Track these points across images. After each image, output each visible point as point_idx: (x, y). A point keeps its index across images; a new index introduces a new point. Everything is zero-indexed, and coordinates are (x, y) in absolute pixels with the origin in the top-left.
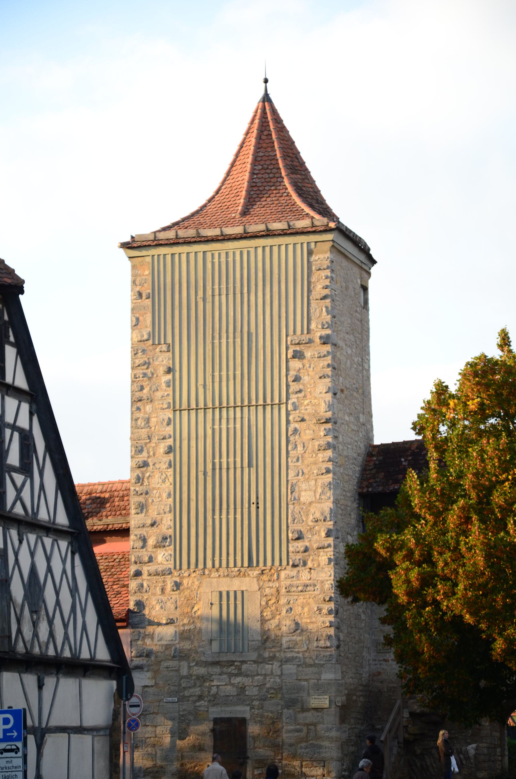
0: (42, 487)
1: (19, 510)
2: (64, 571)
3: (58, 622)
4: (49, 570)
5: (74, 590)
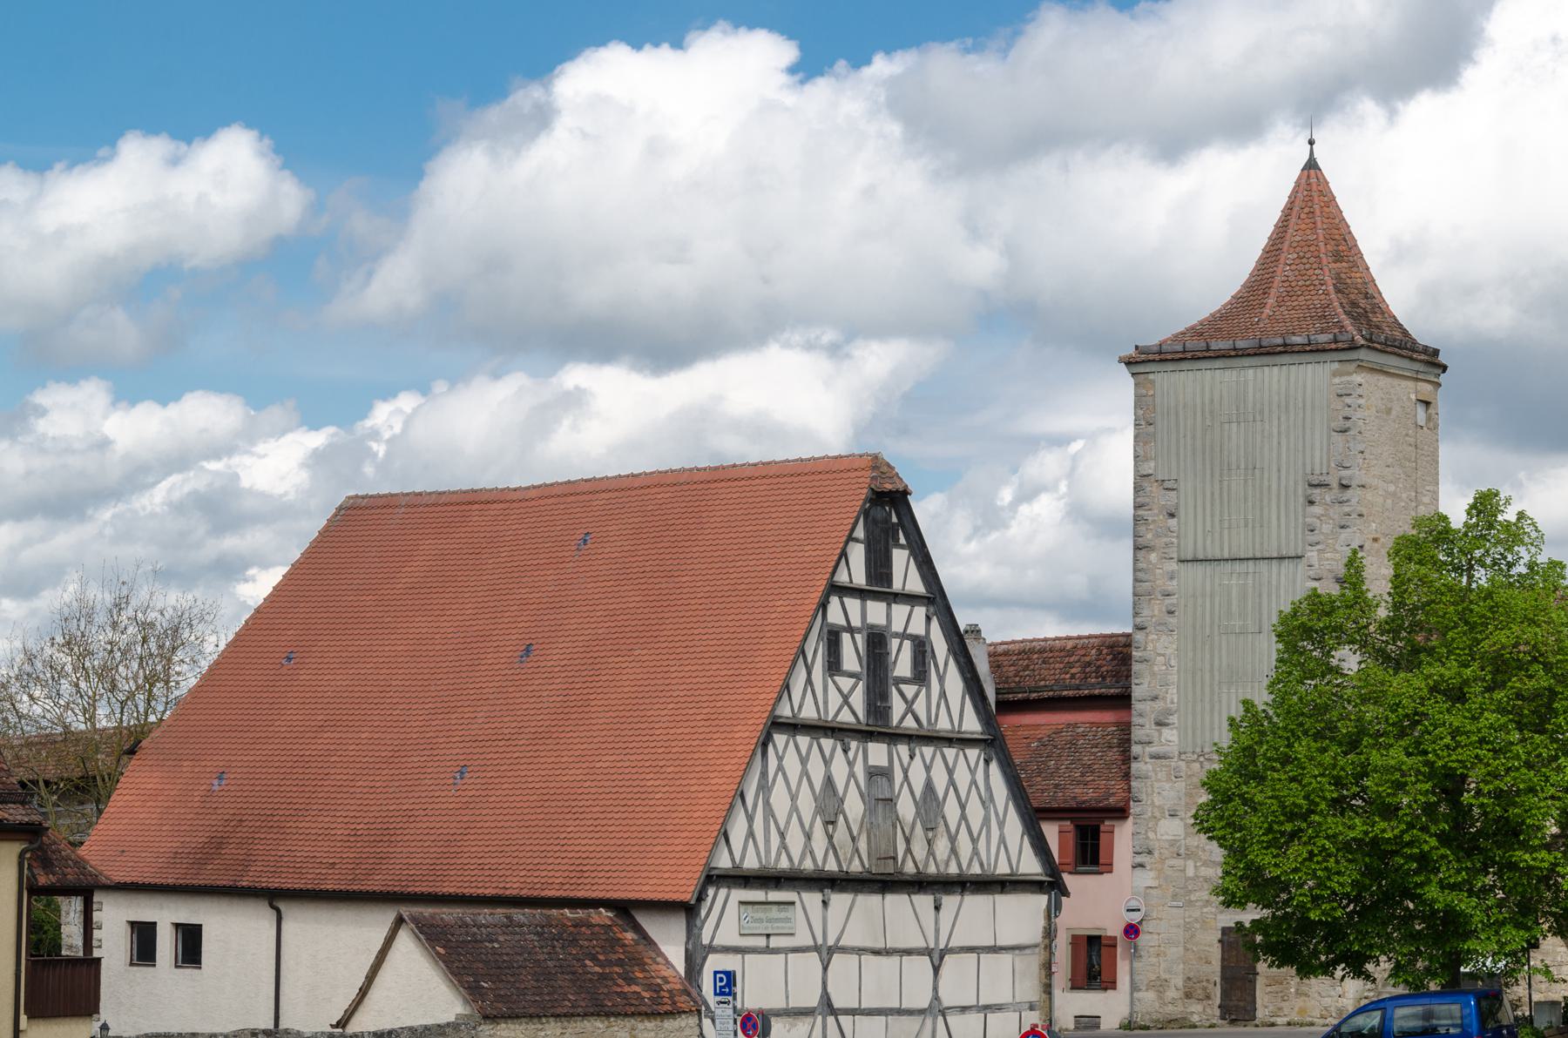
0: (943, 694)
1: (910, 723)
2: (974, 782)
3: (963, 838)
4: (952, 782)
5: (987, 801)
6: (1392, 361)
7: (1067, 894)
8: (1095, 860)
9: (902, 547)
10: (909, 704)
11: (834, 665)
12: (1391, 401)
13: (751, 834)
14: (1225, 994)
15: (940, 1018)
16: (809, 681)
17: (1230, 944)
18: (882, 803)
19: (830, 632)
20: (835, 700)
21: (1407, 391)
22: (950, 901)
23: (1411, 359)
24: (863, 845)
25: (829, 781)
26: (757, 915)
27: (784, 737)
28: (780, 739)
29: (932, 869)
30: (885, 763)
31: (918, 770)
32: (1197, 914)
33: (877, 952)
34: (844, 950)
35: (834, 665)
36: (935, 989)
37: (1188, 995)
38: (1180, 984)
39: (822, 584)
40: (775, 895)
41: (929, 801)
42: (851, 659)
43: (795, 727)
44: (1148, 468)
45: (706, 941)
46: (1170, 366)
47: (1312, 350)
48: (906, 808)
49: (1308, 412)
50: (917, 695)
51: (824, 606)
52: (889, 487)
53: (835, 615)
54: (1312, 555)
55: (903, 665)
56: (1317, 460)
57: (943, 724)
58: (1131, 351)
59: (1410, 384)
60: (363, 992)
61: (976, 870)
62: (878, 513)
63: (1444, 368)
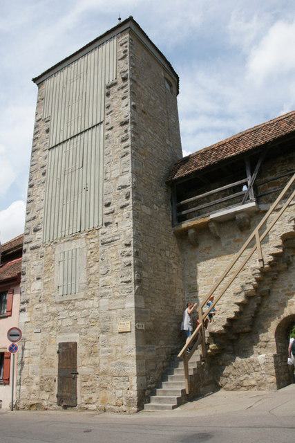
17: (63, 353)
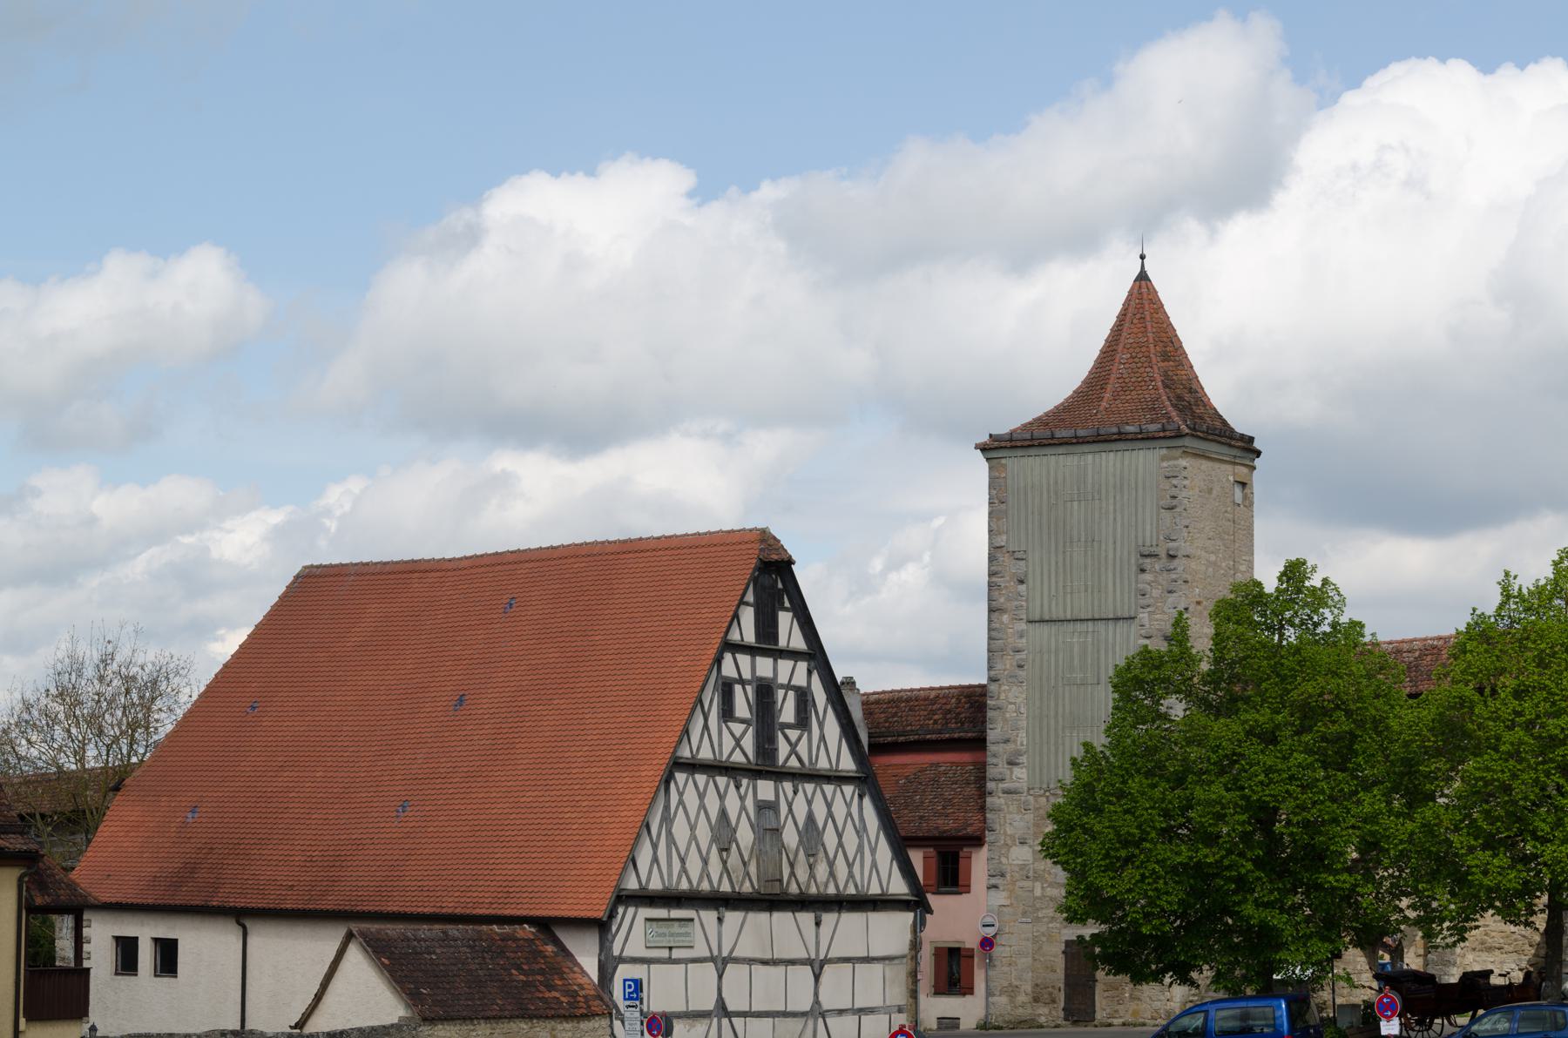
0: (822, 738)
1: (794, 763)
2: (849, 814)
3: (841, 865)
4: (830, 815)
5: (861, 831)
6: (1212, 448)
7: (930, 911)
8: (955, 883)
9: (787, 610)
10: (793, 746)
11: (727, 713)
12: (1211, 481)
13: (655, 860)
14: (1068, 998)
15: (820, 1020)
16: (706, 727)
18: (768, 832)
19: (724, 684)
20: (728, 743)
21: (1227, 473)
22: (829, 918)
23: (1230, 446)
24: (753, 869)
25: (723, 813)
26: (660, 931)
27: (684, 776)
28: (680, 777)
29: (813, 890)
30: (772, 798)
31: (800, 803)
32: (1043, 929)
33: (765, 962)
34: (737, 961)
35: (727, 713)
36: (816, 994)
37: (1036, 1000)
38: (1029, 989)
39: (716, 643)
40: (676, 913)
41: (810, 831)
42: (742, 708)
43: (693, 767)
44: (1001, 540)
45: (616, 952)
46: (1019, 452)
47: (1144, 438)
48: (790, 837)
49: (1140, 491)
50: (799, 739)
51: (718, 661)
52: (775, 557)
53: (728, 669)
54: (1144, 616)
55: (788, 714)
56: (1148, 534)
57: (823, 764)
58: (986, 438)
59: (1229, 467)
60: (318, 998)
61: (851, 890)
62: (766, 580)
63: (1258, 453)
